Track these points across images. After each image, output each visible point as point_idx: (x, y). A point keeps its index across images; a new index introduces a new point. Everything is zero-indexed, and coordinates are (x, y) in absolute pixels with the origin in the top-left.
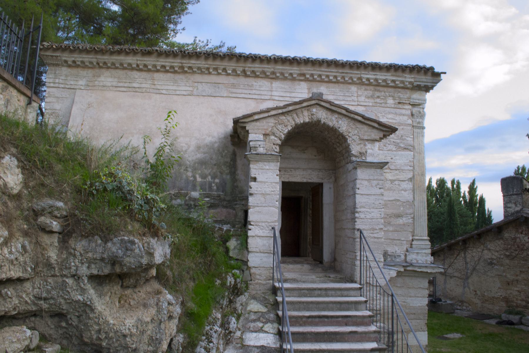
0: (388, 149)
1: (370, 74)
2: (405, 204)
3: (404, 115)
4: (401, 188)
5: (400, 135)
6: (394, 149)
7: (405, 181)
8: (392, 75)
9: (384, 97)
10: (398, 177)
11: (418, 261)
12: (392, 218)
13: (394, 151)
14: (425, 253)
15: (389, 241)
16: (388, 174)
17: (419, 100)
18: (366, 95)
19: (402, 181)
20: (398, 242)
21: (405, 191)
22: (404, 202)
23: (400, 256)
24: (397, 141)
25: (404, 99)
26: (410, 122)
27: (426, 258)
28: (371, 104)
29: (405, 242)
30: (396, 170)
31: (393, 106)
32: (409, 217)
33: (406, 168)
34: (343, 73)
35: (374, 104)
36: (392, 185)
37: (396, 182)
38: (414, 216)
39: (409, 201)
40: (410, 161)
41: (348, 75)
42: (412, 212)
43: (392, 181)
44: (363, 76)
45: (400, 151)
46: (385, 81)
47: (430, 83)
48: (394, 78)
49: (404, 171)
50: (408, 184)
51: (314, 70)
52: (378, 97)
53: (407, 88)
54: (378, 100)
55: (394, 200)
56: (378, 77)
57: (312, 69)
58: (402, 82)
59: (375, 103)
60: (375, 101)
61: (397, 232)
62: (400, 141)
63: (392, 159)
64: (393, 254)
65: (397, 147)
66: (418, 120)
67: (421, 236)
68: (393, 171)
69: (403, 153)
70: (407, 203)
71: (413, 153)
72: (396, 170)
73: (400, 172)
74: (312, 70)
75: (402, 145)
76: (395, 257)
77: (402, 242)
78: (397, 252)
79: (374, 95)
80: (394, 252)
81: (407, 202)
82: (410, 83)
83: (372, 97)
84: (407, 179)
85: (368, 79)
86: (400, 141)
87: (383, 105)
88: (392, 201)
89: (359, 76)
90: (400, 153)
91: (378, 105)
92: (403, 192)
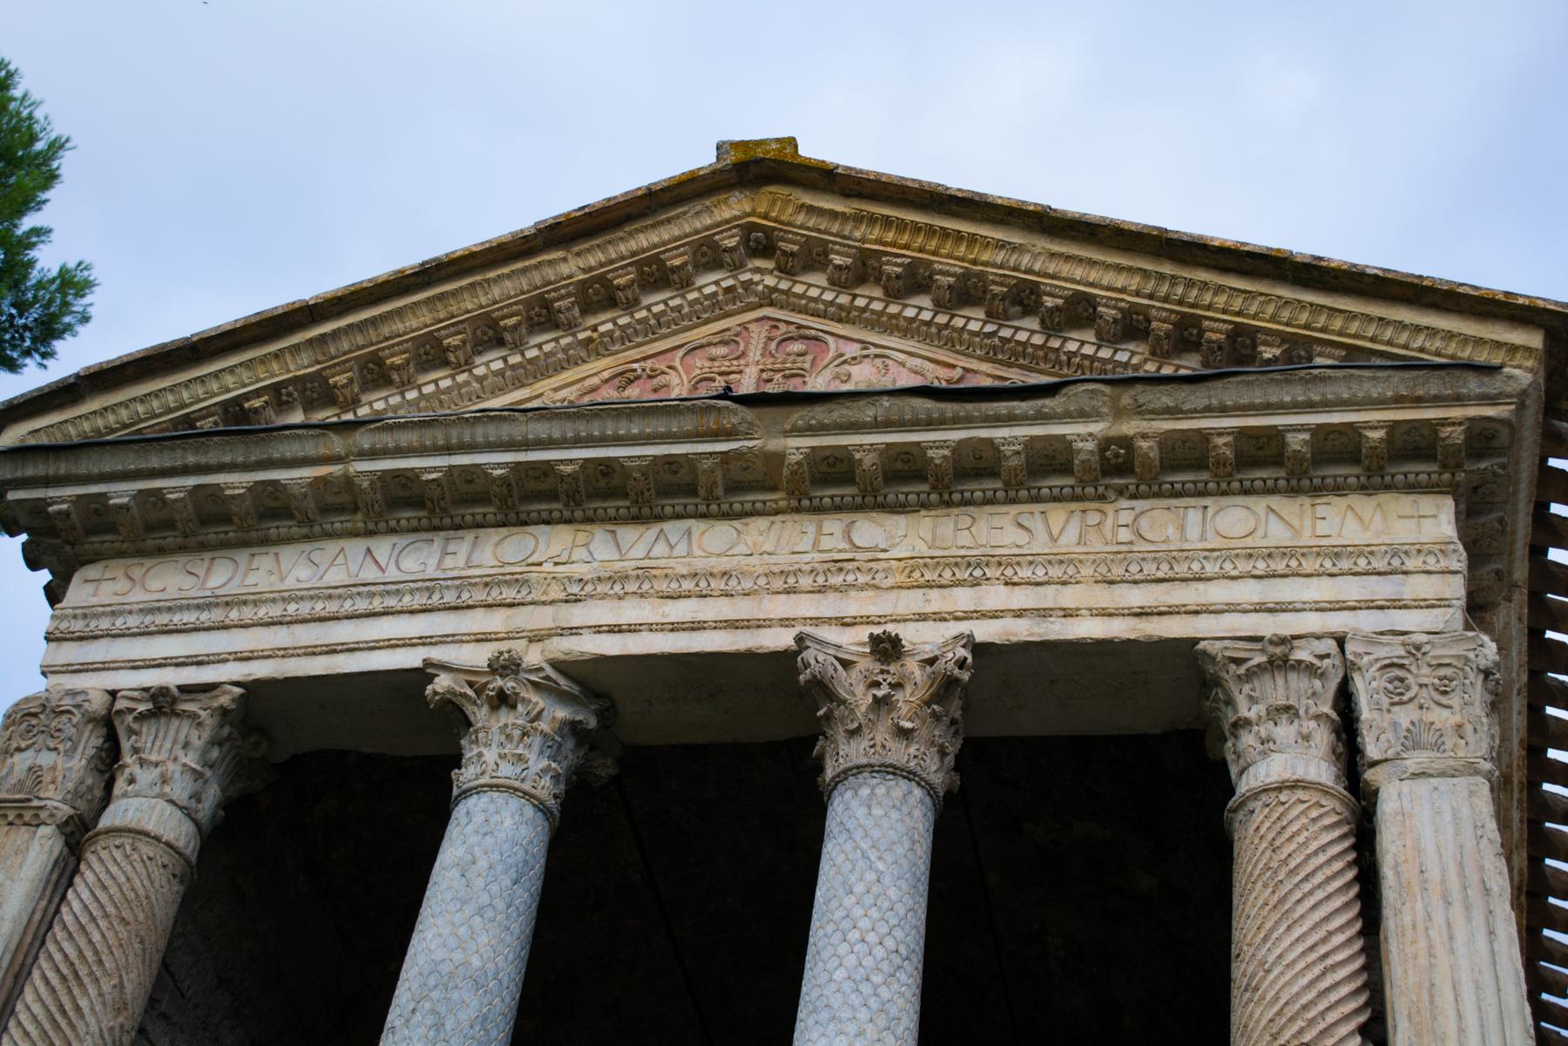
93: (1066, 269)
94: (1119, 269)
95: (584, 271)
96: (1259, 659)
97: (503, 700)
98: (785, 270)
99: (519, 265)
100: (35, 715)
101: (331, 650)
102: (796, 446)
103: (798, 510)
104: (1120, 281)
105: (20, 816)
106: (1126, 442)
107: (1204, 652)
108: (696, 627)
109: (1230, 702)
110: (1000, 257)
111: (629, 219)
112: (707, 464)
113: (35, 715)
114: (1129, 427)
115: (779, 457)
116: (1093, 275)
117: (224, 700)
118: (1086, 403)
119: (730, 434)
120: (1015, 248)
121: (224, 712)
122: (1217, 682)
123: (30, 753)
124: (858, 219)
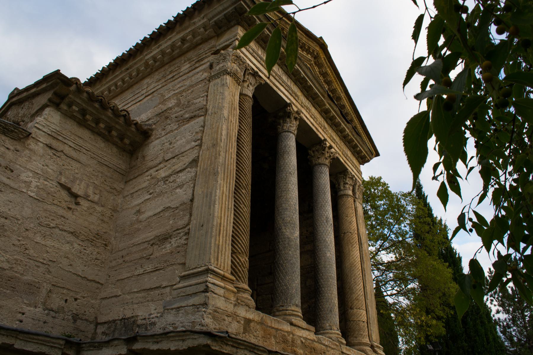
0: (167, 131)
1: (154, 50)
2: (177, 211)
3: (198, 73)
4: (176, 185)
5: (186, 103)
6: (175, 127)
7: (184, 169)
8: (178, 33)
9: (178, 67)
10: (173, 168)
11: (176, 328)
12: (155, 247)
13: (175, 130)
14: (193, 305)
15: (143, 294)
16: (162, 170)
17: (227, 41)
18: (157, 79)
19: (181, 171)
20: (157, 292)
21: (180, 186)
22: (177, 208)
23: (154, 324)
24: (181, 112)
25: (204, 54)
26: (206, 75)
27: (192, 318)
28: (160, 86)
29: (168, 290)
30: (174, 158)
31: (186, 71)
32: (182, 234)
33: (188, 147)
34: (128, 69)
35: (164, 84)
36: (165, 186)
37: (172, 179)
38: (189, 229)
39: (184, 203)
40: (197, 133)
41: (133, 68)
42: (186, 222)
43: (165, 179)
44: (147, 58)
45: (183, 125)
46: (173, 47)
47: (230, 6)
48: (181, 35)
49: (184, 154)
50: (189, 172)
51: (102, 86)
52: (171, 72)
53: (209, 38)
54: (171, 76)
55: (162, 211)
56: (163, 47)
57: (100, 86)
58: (194, 34)
59: (165, 81)
60: (166, 80)
61: (157, 272)
62: (185, 111)
63: (170, 144)
64: (144, 322)
65: (181, 121)
66: (217, 68)
67: (195, 268)
68: (170, 161)
69: (187, 125)
70: (181, 207)
71: (202, 118)
72: (174, 158)
73: (178, 158)
74: (100, 88)
75: (187, 116)
76: (146, 329)
77: (163, 291)
78: (152, 316)
79: (166, 74)
80: (147, 317)
81: (181, 205)
82: (205, 27)
83: (164, 77)
84: (187, 164)
85: (154, 59)
86: (185, 111)
87: (176, 77)
88: (159, 213)
89: (144, 61)
90: (182, 128)
91: (169, 81)
92: (178, 190)
93: (345, 101)
94: (349, 107)
95: (305, 42)
96: (350, 176)
97: (296, 119)
98: (315, 63)
99: (303, 34)
100: (238, 58)
101: (277, 87)
102: (328, 106)
103: (319, 113)
104: (349, 108)
105: (237, 80)
106: (349, 135)
107: (348, 172)
108: (313, 125)
109: (346, 179)
110: (340, 91)
111: (312, 38)
112: (320, 99)
113: (238, 58)
114: (350, 134)
115: (325, 105)
116: (347, 105)
117: (263, 82)
118: (350, 128)
119: (324, 97)
120: (342, 92)
121: (261, 83)
122: (346, 176)
123: (236, 65)
124: (329, 68)
